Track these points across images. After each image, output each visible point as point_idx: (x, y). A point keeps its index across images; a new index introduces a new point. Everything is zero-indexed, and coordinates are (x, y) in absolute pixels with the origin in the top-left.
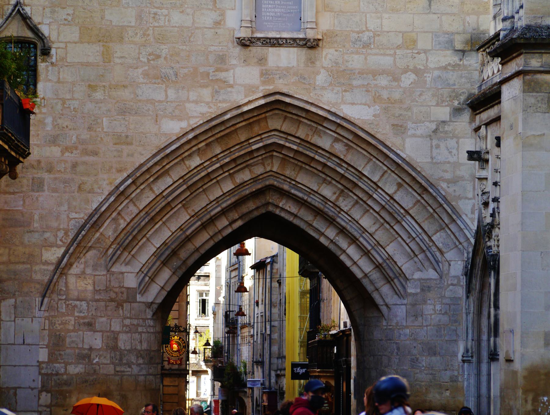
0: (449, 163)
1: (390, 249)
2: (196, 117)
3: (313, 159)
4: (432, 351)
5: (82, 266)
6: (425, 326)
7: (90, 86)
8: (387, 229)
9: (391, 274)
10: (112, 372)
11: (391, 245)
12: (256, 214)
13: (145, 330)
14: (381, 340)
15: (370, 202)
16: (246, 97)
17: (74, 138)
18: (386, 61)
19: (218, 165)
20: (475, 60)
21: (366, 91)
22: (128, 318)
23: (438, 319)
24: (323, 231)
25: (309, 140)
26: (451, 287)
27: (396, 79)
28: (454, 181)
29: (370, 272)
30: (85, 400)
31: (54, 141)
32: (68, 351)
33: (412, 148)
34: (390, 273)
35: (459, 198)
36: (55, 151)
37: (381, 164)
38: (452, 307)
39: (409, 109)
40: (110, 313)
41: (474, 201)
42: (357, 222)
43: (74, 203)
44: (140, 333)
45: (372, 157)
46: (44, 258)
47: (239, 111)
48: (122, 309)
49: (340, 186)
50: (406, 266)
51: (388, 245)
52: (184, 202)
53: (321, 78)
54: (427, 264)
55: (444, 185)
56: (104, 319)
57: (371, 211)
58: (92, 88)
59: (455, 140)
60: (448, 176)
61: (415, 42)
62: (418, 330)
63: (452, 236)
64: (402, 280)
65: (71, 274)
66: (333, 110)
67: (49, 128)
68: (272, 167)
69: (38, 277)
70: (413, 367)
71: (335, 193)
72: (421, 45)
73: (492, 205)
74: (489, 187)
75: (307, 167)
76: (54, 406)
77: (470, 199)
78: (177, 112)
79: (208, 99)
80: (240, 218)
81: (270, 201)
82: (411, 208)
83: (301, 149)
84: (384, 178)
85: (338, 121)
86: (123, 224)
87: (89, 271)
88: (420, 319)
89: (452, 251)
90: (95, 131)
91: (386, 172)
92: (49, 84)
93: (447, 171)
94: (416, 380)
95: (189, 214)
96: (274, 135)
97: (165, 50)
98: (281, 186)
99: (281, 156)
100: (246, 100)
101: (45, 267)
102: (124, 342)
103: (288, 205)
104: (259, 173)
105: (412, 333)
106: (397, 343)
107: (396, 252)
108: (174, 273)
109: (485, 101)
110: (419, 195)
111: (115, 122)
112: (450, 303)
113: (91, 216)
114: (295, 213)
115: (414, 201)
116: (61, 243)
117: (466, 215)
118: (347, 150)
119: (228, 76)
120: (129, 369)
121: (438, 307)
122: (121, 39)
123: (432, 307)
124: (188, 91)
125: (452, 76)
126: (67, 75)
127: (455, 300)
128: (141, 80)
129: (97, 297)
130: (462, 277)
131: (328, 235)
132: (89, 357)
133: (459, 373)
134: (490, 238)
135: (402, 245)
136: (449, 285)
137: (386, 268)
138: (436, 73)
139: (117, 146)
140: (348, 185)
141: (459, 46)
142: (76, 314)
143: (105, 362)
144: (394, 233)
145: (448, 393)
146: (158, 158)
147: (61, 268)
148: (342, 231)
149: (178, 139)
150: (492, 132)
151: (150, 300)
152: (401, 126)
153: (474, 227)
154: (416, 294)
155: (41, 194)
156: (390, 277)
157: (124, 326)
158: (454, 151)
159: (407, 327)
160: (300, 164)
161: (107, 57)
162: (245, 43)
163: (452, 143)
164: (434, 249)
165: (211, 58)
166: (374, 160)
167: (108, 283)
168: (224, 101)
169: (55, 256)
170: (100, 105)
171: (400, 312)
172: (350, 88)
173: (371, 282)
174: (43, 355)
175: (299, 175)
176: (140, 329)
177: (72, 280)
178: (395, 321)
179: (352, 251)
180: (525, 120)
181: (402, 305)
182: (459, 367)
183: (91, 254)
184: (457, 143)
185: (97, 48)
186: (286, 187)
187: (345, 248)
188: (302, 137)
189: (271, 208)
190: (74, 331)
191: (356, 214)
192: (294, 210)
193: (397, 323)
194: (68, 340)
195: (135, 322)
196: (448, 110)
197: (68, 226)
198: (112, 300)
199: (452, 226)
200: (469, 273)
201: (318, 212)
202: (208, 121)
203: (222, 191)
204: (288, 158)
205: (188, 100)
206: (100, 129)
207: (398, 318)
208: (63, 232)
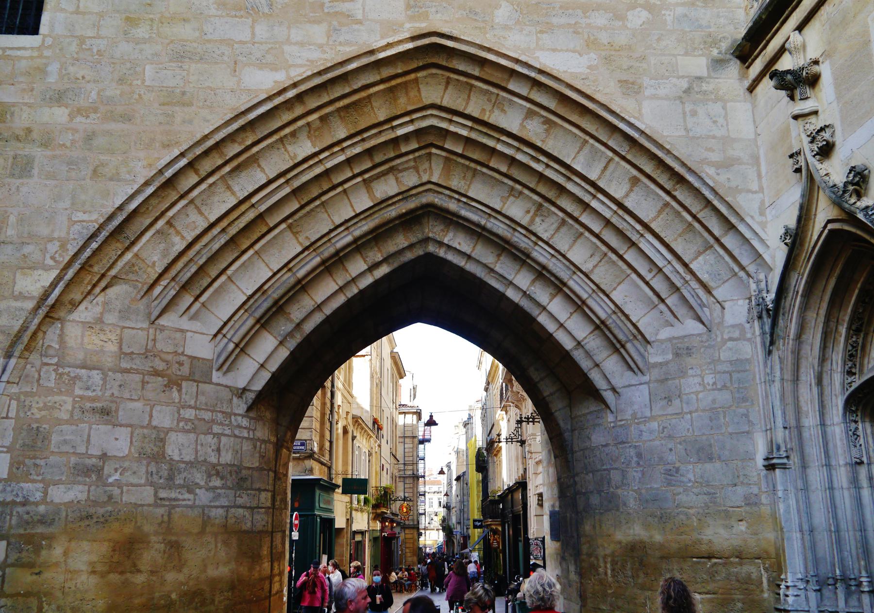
0: (714, 137)
2: (301, 66)
3: (493, 151)
4: (705, 454)
5: (99, 309)
6: (686, 413)
7: (128, 19)
8: (614, 262)
9: (621, 336)
10: (151, 500)
11: (619, 288)
12: (409, 256)
13: (228, 432)
14: (607, 445)
15: (585, 219)
16: (382, 38)
17: (94, 95)
19: (342, 158)
21: (574, 32)
22: (190, 407)
23: (710, 398)
24: (510, 278)
25: (486, 119)
26: (730, 344)
27: (621, 17)
28: (727, 164)
29: (585, 338)
31: (58, 98)
32: (53, 459)
35: (737, 190)
36: (60, 114)
37: (603, 148)
38: (735, 376)
39: (643, 58)
40: (150, 395)
41: (761, 195)
42: (564, 256)
43: (83, 197)
44: (218, 436)
45: (587, 138)
46: (18, 288)
47: (372, 59)
48: (180, 391)
49: (536, 197)
50: (645, 319)
51: (615, 289)
52: (290, 221)
54: (681, 311)
55: (711, 171)
56: (138, 405)
57: (587, 234)
58: (131, 21)
59: (719, 104)
60: (715, 157)
62: (674, 421)
63: (727, 258)
64: (639, 346)
65: (74, 321)
66: (523, 58)
67: (52, 79)
68: (431, 175)
70: (669, 484)
71: (528, 212)
75: (484, 170)
76: (12, 565)
77: (755, 192)
78: (270, 58)
79: (322, 40)
80: (385, 260)
81: (431, 235)
82: (654, 219)
83: (474, 136)
84: (608, 172)
85: (533, 74)
87: (110, 318)
88: (676, 402)
89: (726, 284)
90: (131, 84)
91: (611, 160)
92: (61, 16)
93: (710, 150)
94: (678, 506)
95: (301, 244)
96: (432, 115)
98: (445, 205)
99: (444, 154)
100: (383, 43)
101: (18, 304)
102: (179, 447)
103: (458, 240)
104: (411, 184)
105: (664, 428)
106: (635, 447)
107: (627, 299)
108: (281, 343)
110: (668, 193)
111: (165, 71)
112: (730, 369)
113: (111, 218)
114: (468, 252)
115: (660, 205)
116: (51, 263)
117: (752, 217)
118: (547, 130)
120: (187, 496)
121: (709, 379)
123: (697, 380)
124: (289, 28)
127: (740, 365)
128: (213, 12)
129: (124, 365)
130: (748, 326)
131: (518, 284)
132: (99, 471)
133: (760, 489)
135: (638, 286)
136: (724, 342)
137: (612, 326)
138: (680, 10)
139: (166, 107)
140: (551, 187)
142: (78, 392)
143: (134, 480)
144: (625, 267)
145: (742, 527)
146: (235, 126)
148: (542, 274)
149: (269, 98)
151: (241, 384)
152: (633, 83)
154: (666, 363)
155: (25, 180)
156: (619, 341)
157: (179, 420)
158: (721, 121)
159: (652, 418)
160: (473, 165)
163: (716, 108)
164: (694, 284)
166: (591, 141)
167: (150, 344)
168: (347, 43)
169: (39, 285)
170: (143, 46)
172: (549, 28)
173: (588, 354)
175: (472, 186)
176: (216, 429)
178: (630, 412)
179: (558, 307)
181: (641, 384)
182: (759, 479)
184: (724, 108)
186: (453, 206)
187: (544, 304)
188: (476, 114)
189: (431, 248)
190: (67, 422)
192: (466, 247)
193: (634, 416)
194: (55, 438)
195: (207, 416)
197: (68, 233)
198: (156, 373)
201: (504, 247)
202: (320, 73)
203: (354, 211)
204: (454, 158)
205: (288, 41)
206: (139, 82)
207: (636, 407)
208: (58, 244)
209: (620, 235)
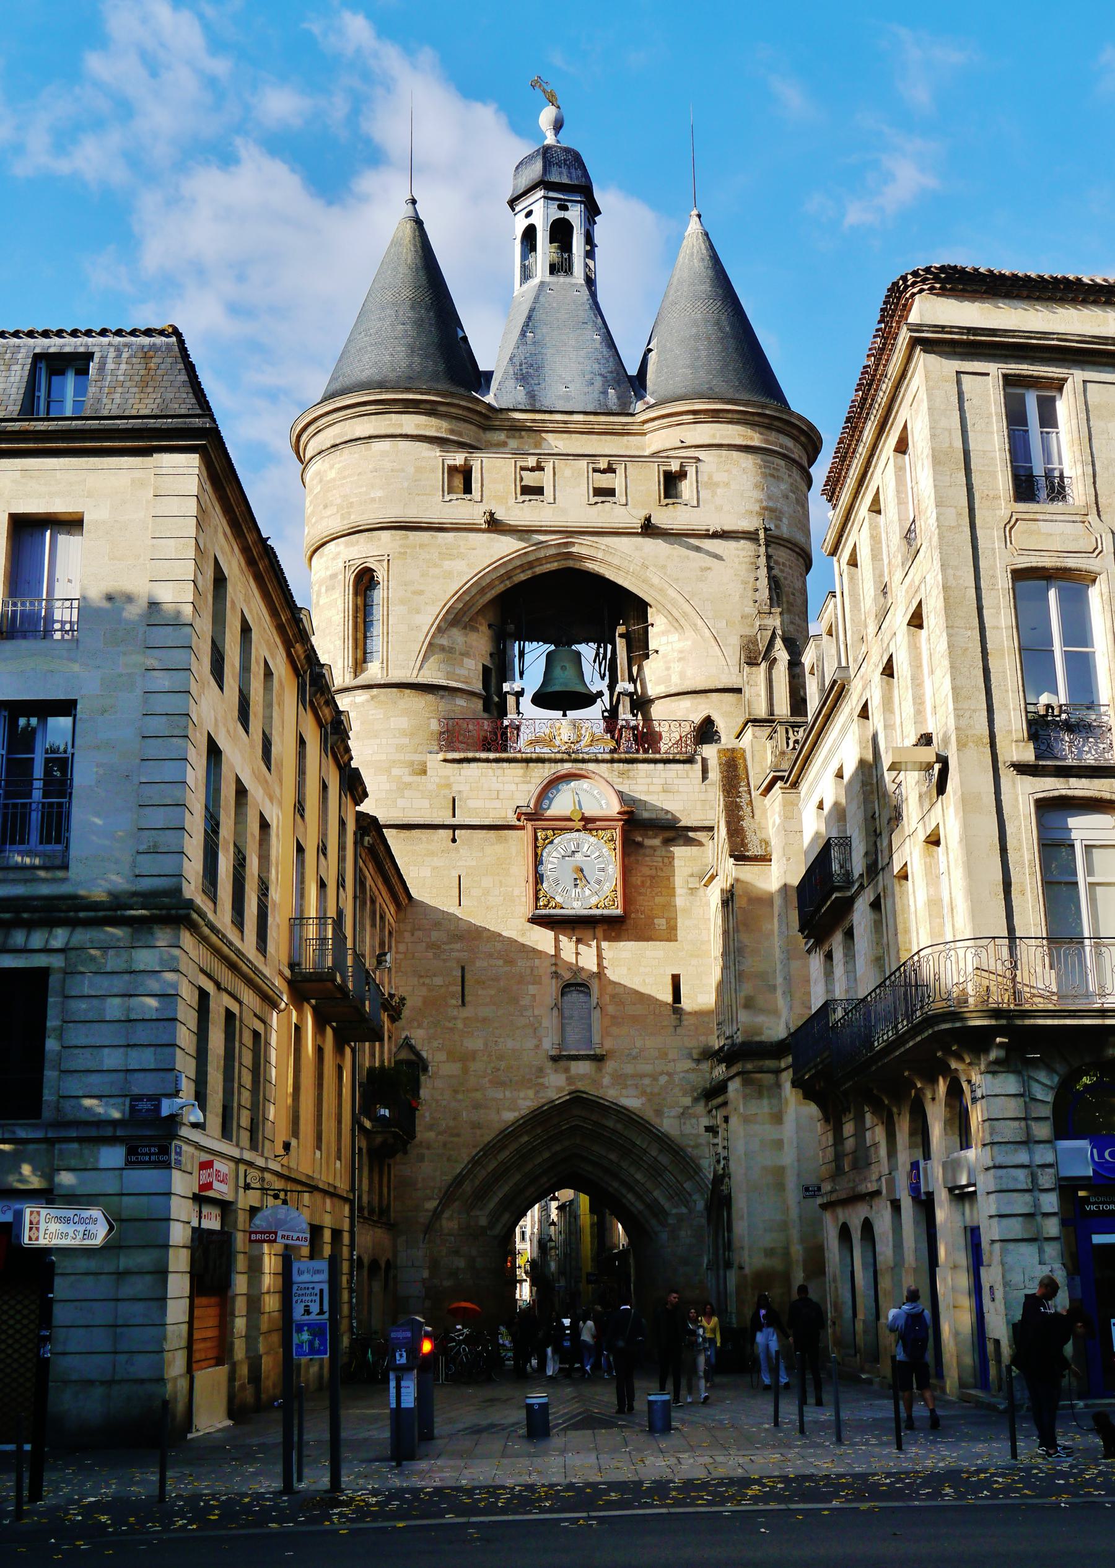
1: (656, 1193)
18: (648, 1068)
20: (705, 1066)
30: (456, 1305)
31: (430, 1128)
33: (668, 1125)
34: (657, 1211)
35: (700, 1158)
36: (431, 1135)
39: (664, 1099)
50: (667, 1206)
53: (606, 1081)
58: (456, 1092)
60: (692, 1143)
61: (666, 1054)
67: (427, 1119)
69: (422, 1220)
72: (670, 1057)
73: (722, 1162)
74: (720, 1150)
86: (477, 1182)
97: (503, 1065)
109: (714, 1093)
119: (545, 1081)
122: (474, 1059)
125: (692, 1077)
126: (439, 1083)
134: (722, 1184)
138: (682, 1075)
141: (695, 1057)
147: (437, 1214)
148: (623, 1183)
150: (720, 1114)
153: (711, 1176)
161: (465, 1070)
162: (555, 1059)
163: (694, 1121)
165: (534, 1070)
171: (664, 1236)
172: (625, 1087)
174: (426, 1274)
177: (444, 1223)
179: (630, 1196)
180: (744, 1104)
183: (457, 1203)
185: (459, 1065)
191: (632, 1170)
196: (690, 1099)
199: (697, 1178)
200: (709, 1208)
209: (655, 1171)
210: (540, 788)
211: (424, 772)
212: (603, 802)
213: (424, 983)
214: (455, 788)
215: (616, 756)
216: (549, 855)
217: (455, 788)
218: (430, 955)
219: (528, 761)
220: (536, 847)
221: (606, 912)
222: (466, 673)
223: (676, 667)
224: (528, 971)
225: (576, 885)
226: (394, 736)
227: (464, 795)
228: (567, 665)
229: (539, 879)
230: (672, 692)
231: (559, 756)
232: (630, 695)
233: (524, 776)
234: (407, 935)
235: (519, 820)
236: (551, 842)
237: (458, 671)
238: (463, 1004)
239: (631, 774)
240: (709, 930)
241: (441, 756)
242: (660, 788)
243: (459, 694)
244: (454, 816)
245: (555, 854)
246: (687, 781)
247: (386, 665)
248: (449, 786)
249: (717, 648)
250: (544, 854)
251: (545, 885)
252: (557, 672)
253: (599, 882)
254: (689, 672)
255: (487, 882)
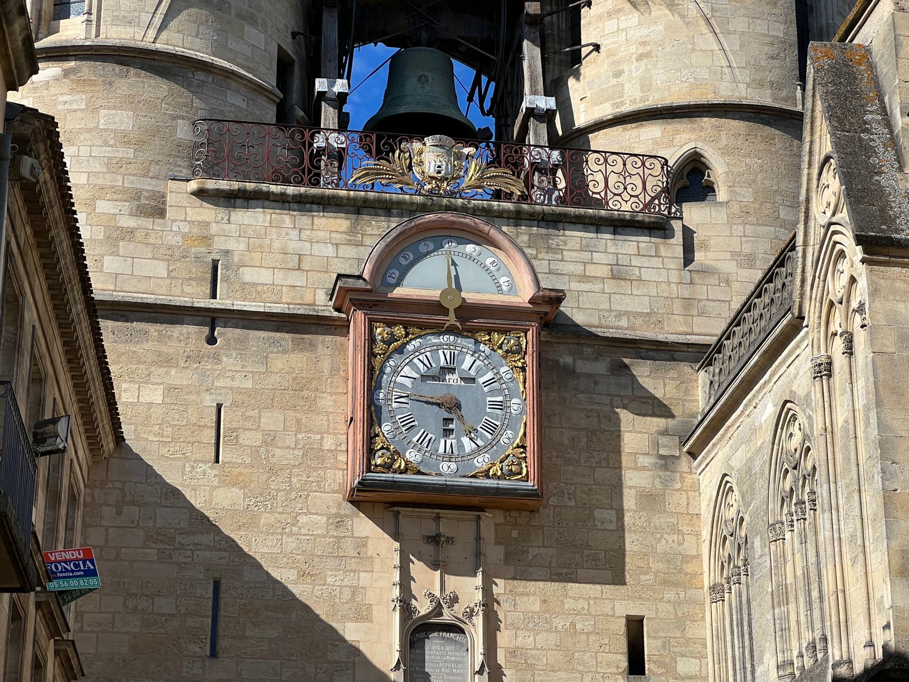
210: (383, 244)
211: (159, 212)
212: (502, 280)
213: (135, 610)
214: (219, 244)
215: (525, 206)
216: (396, 371)
217: (219, 244)
218: (152, 553)
219: (358, 208)
220: (372, 355)
221: (504, 484)
222: (248, 51)
223: (634, 70)
224: (347, 594)
225: (447, 432)
226: (106, 144)
227: (236, 259)
228: (429, 75)
229: (374, 415)
230: (627, 108)
231: (418, 199)
232: (547, 116)
233: (352, 231)
234: (107, 512)
235: (338, 310)
236: (400, 350)
237: (232, 45)
238: (214, 654)
239: (553, 242)
240: (698, 535)
241: (193, 185)
242: (604, 271)
243: (233, 84)
244: (214, 296)
245: (407, 371)
246: (656, 262)
247: (94, 20)
248: (206, 239)
249: (710, 36)
250: (388, 370)
251: (386, 427)
252: (412, 85)
253: (492, 429)
254: (659, 77)
255: (271, 420)
